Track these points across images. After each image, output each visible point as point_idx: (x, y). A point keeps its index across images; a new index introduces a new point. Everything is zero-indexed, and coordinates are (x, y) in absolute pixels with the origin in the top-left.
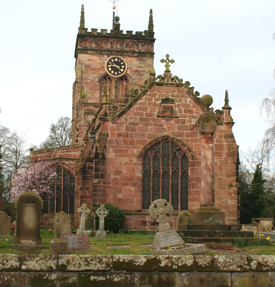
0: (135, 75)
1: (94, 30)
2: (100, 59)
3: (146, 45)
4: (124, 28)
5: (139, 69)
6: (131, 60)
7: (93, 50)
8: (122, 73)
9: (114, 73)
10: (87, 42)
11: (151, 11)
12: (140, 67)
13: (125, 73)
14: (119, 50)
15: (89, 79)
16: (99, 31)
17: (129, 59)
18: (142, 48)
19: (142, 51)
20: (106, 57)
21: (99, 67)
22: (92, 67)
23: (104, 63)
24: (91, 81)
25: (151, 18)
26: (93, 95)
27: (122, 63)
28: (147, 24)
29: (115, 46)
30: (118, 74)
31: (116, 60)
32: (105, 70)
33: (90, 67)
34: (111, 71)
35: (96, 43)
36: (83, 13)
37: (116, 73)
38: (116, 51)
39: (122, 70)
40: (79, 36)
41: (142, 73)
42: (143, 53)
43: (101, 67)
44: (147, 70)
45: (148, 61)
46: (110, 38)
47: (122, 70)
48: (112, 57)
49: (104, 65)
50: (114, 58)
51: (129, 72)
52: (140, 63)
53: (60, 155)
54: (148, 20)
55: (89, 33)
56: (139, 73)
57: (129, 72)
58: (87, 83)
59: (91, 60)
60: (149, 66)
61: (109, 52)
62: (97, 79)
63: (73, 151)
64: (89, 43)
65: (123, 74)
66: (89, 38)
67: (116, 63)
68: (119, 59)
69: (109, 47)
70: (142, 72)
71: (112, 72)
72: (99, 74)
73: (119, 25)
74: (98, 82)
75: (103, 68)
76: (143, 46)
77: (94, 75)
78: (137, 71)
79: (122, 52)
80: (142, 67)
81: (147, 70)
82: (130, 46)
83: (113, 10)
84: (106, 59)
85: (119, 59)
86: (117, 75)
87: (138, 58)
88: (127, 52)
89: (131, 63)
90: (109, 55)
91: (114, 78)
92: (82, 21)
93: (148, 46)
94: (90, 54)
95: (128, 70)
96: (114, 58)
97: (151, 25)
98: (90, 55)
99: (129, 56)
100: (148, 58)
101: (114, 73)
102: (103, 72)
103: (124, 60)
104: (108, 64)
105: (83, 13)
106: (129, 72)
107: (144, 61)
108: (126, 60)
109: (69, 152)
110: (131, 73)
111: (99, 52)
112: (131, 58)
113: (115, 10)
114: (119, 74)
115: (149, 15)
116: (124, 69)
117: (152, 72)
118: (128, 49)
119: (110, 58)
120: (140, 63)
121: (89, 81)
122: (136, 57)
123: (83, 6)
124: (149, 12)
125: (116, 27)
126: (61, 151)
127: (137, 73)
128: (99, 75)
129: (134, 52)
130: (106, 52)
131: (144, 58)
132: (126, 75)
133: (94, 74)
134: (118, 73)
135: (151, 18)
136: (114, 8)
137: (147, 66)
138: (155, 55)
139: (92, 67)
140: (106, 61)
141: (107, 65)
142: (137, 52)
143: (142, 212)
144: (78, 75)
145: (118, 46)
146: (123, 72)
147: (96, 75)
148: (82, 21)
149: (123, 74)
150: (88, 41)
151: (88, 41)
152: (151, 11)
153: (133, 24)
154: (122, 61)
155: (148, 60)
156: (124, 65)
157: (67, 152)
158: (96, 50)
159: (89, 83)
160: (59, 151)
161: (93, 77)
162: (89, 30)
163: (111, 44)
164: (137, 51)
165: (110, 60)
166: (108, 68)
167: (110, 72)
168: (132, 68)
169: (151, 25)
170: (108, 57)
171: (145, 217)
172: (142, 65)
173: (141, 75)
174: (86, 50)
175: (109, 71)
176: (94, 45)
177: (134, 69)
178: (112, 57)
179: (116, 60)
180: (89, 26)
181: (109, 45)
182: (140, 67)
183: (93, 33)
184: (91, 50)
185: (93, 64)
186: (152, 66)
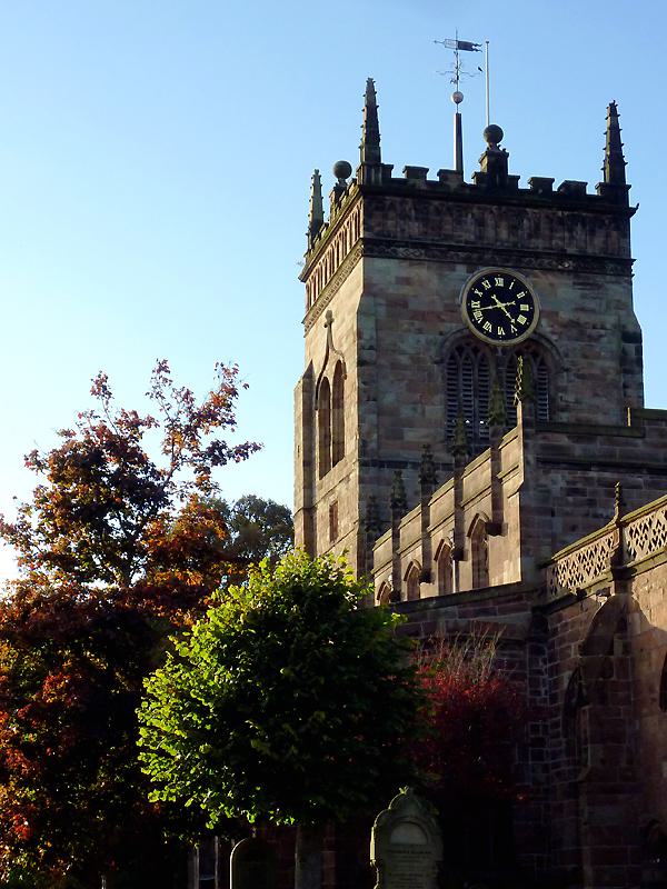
0: (569, 339)
1: (416, 173)
2: (441, 276)
4: (523, 170)
5: (583, 318)
6: (552, 285)
7: (415, 245)
8: (522, 329)
9: (495, 330)
11: (613, 108)
12: (583, 310)
13: (535, 332)
15: (404, 353)
16: (432, 176)
17: (545, 280)
18: (580, 241)
19: (590, 251)
20: (461, 270)
21: (439, 308)
22: (413, 306)
23: (456, 294)
24: (412, 358)
26: (419, 410)
27: (521, 295)
28: (600, 156)
29: (490, 233)
30: (509, 336)
31: (500, 282)
32: (460, 320)
33: (405, 305)
34: (483, 322)
35: (425, 221)
36: (372, 110)
37: (501, 331)
38: (498, 252)
39: (522, 320)
41: (594, 332)
42: (595, 259)
43: (446, 305)
44: (610, 320)
45: (614, 290)
49: (458, 301)
51: (546, 328)
52: (583, 296)
53: (451, 626)
54: (603, 141)
57: (549, 329)
58: (395, 366)
59: (407, 281)
60: (617, 308)
61: (474, 255)
62: (433, 351)
63: (503, 612)
66: (398, 199)
67: (504, 295)
70: (594, 328)
71: (488, 326)
72: (441, 334)
73: (505, 155)
74: (436, 363)
75: (453, 309)
76: (592, 233)
77: (422, 338)
79: (518, 257)
80: (593, 311)
84: (462, 278)
85: (508, 279)
86: (504, 338)
87: (577, 277)
88: (537, 255)
89: (553, 297)
90: (472, 266)
91: (494, 349)
93: (608, 236)
94: (405, 259)
95: (544, 322)
96: (491, 278)
97: (615, 162)
98: (405, 264)
99: (546, 270)
100: (613, 279)
101: (495, 330)
102: (454, 326)
103: (528, 283)
104: (472, 297)
105: (372, 110)
106: (549, 329)
107: (600, 287)
108: (536, 283)
109: (486, 612)
110: (553, 333)
111: (440, 252)
112: (551, 278)
113: (461, 108)
115: (607, 123)
116: (530, 315)
117: (630, 329)
118: (539, 244)
119: (477, 275)
120: (583, 296)
121: (404, 360)
122: (569, 272)
123: (370, 83)
124: (606, 113)
125: (497, 160)
126: (455, 609)
127: (574, 332)
128: (441, 338)
129: (562, 255)
131: (599, 279)
132: (536, 337)
133: (420, 331)
134: (507, 329)
136: (458, 100)
137: (608, 307)
139: (413, 306)
141: (469, 301)
142: (571, 257)
144: (366, 336)
145: (504, 234)
147: (431, 337)
150: (394, 214)
151: (394, 214)
153: (557, 154)
154: (520, 287)
156: (528, 300)
157: (477, 614)
159: (406, 368)
160: (450, 609)
162: (398, 174)
163: (481, 223)
164: (570, 250)
165: (478, 285)
167: (480, 327)
168: (557, 314)
169: (615, 162)
170: (470, 271)
172: (592, 305)
173: (590, 337)
174: (389, 244)
175: (475, 323)
176: (415, 228)
177: (565, 316)
178: (485, 270)
179: (500, 282)
180: (397, 157)
182: (583, 310)
183: (412, 181)
184: (406, 245)
186: (627, 305)
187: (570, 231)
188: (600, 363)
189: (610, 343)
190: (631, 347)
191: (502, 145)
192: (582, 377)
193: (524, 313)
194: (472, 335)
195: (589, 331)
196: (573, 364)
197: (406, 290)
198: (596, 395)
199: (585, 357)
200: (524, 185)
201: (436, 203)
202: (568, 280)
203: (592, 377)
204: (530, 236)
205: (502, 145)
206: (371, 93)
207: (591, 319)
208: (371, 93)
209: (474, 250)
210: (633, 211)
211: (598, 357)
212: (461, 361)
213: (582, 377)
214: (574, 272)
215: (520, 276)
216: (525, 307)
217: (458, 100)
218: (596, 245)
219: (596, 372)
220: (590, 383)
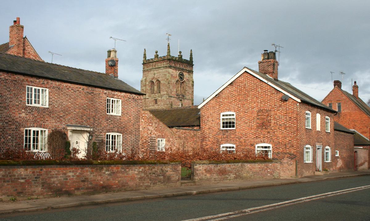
4: (184, 58)
5: (189, 79)
11: (191, 50)
12: (189, 78)
22: (173, 76)
29: (180, 66)
35: (174, 64)
44: (191, 79)
58: (172, 84)
61: (179, 69)
68: (182, 73)
71: (180, 79)
73: (182, 56)
81: (191, 79)
90: (179, 71)
97: (191, 58)
103: (184, 73)
118: (185, 68)
121: (172, 83)
131: (190, 74)
133: (174, 79)
138: (193, 73)
139: (173, 76)
140: (178, 74)
152: (191, 50)
163: (179, 65)
164: (188, 70)
169: (191, 58)
172: (189, 77)
176: (173, 65)
186: (192, 78)
189: (191, 82)
190: (193, 83)
191: (182, 54)
192: (188, 87)
205: (182, 54)
210: (194, 65)
213: (188, 87)
214: (188, 73)
218: (188, 68)
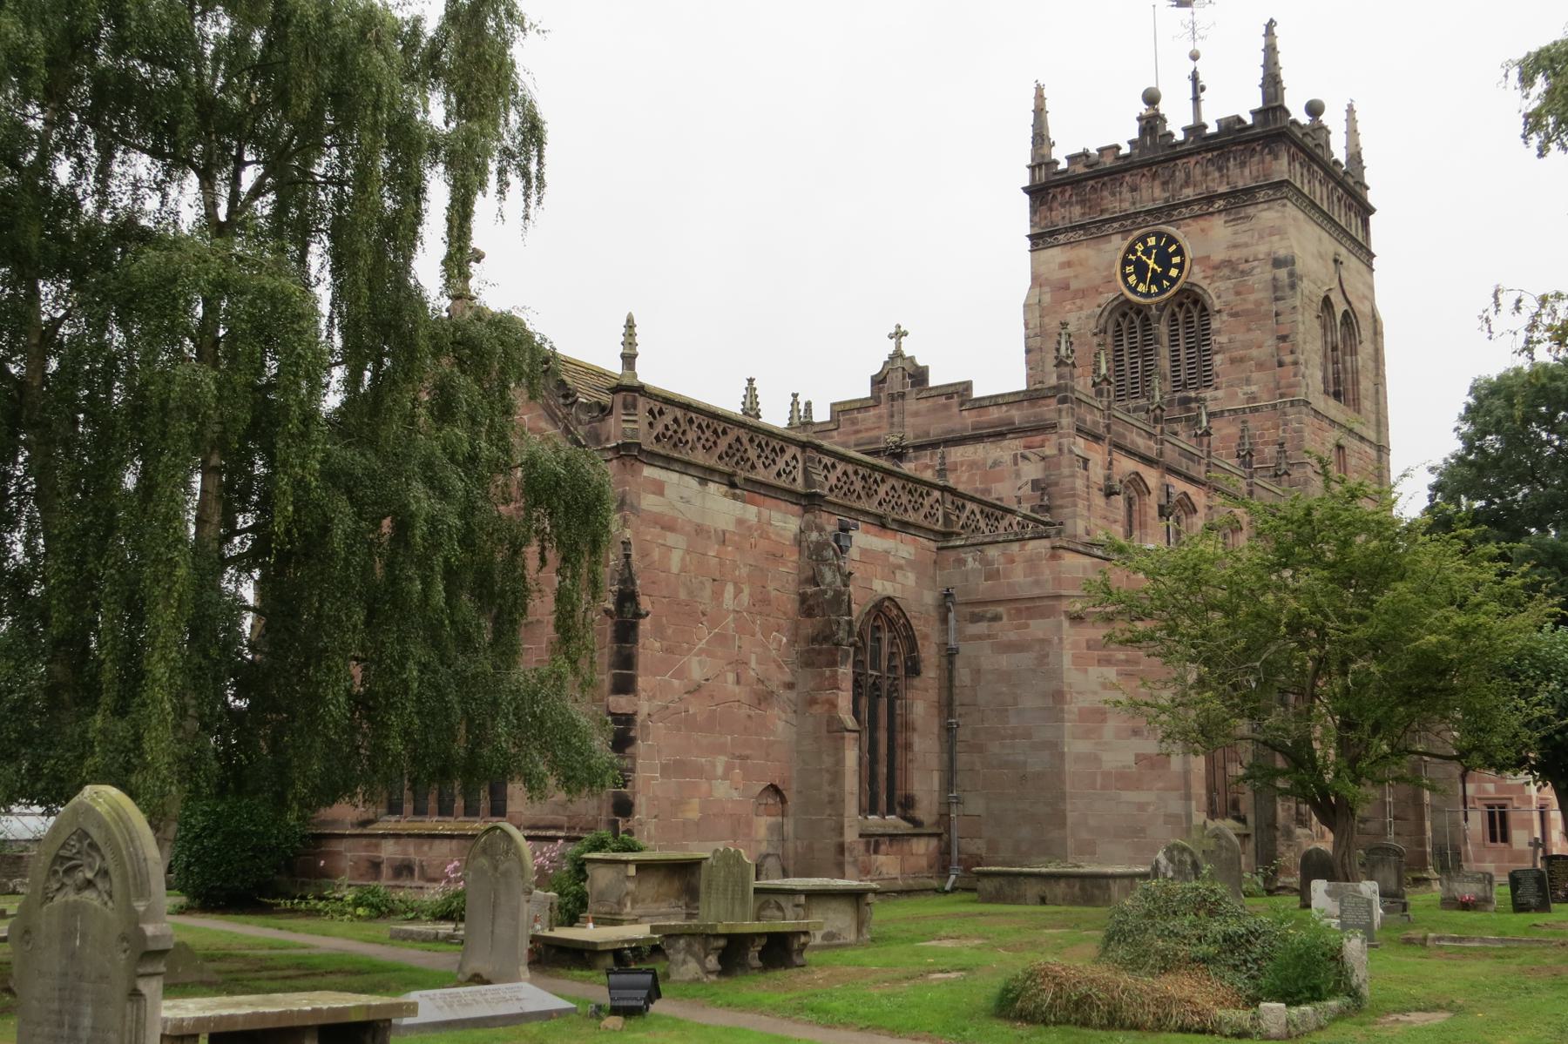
0: (1223, 278)
3: (1256, 159)
5: (1235, 255)
7: (1073, 229)
8: (1173, 281)
10: (1055, 205)
12: (1235, 246)
14: (1160, 204)
19: (1240, 185)
22: (1074, 285)
23: (1111, 265)
25: (1270, 51)
30: (1162, 291)
33: (1067, 287)
35: (1082, 202)
37: (1154, 289)
38: (1149, 212)
40: (1037, 193)
41: (1246, 267)
46: (1126, 170)
47: (1174, 272)
48: (1137, 233)
50: (1143, 239)
54: (1260, 58)
55: (1065, 171)
56: (1234, 270)
59: (1069, 264)
60: (1271, 235)
61: (1126, 221)
62: (1092, 324)
64: (1063, 205)
65: (1175, 288)
68: (1159, 235)
69: (1126, 205)
75: (1109, 280)
76: (1243, 164)
77: (1084, 313)
78: (1228, 263)
79: (1168, 211)
80: (1246, 245)
82: (1199, 178)
83: (1191, 65)
84: (1118, 245)
85: (1159, 235)
86: (1157, 294)
88: (1187, 204)
90: (1125, 232)
92: (1040, 137)
95: (1196, 269)
96: (1143, 239)
100: (1265, 206)
102: (1111, 296)
104: (1126, 262)
107: (1248, 217)
108: (1189, 236)
111: (1093, 230)
112: (1202, 223)
114: (1166, 291)
115: (1262, 43)
116: (1180, 267)
118: (1189, 193)
120: (1236, 233)
122: (1220, 212)
127: (1226, 272)
129: (1210, 199)
130: (1116, 225)
131: (1251, 211)
133: (1081, 308)
134: (1160, 286)
135: (1270, 51)
136: (1195, 57)
137: (1261, 237)
139: (1074, 285)
140: (1120, 255)
142: (1221, 196)
143: (380, 825)
145: (1158, 192)
146: (1178, 277)
148: (1040, 137)
149: (1175, 288)
152: (1270, 26)
154: (1172, 240)
155: (1265, 214)
156: (1180, 252)
158: (1082, 227)
161: (1082, 318)
162: (1063, 165)
163: (1134, 189)
164: (1223, 189)
165: (1131, 249)
166: (1125, 276)
167: (1133, 290)
168: (1208, 257)
170: (1124, 239)
171: (377, 846)
174: (1052, 234)
177: (1218, 256)
178: (1137, 233)
181: (1127, 195)
182: (1235, 246)
184: (1066, 230)
185: (1076, 277)
187: (1220, 169)
188: (1252, 297)
190: (1282, 273)
193: (1176, 266)
194: (1128, 301)
195: (1241, 267)
196: (1227, 304)
197: (1068, 272)
198: (1249, 330)
199: (1238, 293)
200: (1179, 136)
201: (1091, 182)
202: (1218, 222)
203: (1247, 313)
204: (1182, 187)
206: (1040, 96)
207: (1244, 253)
208: (1040, 96)
209: (1127, 217)
211: (1252, 291)
212: (1124, 326)
214: (1225, 210)
215: (1171, 230)
216: (1176, 260)
217: (1195, 57)
219: (1250, 306)
220: (1242, 319)
